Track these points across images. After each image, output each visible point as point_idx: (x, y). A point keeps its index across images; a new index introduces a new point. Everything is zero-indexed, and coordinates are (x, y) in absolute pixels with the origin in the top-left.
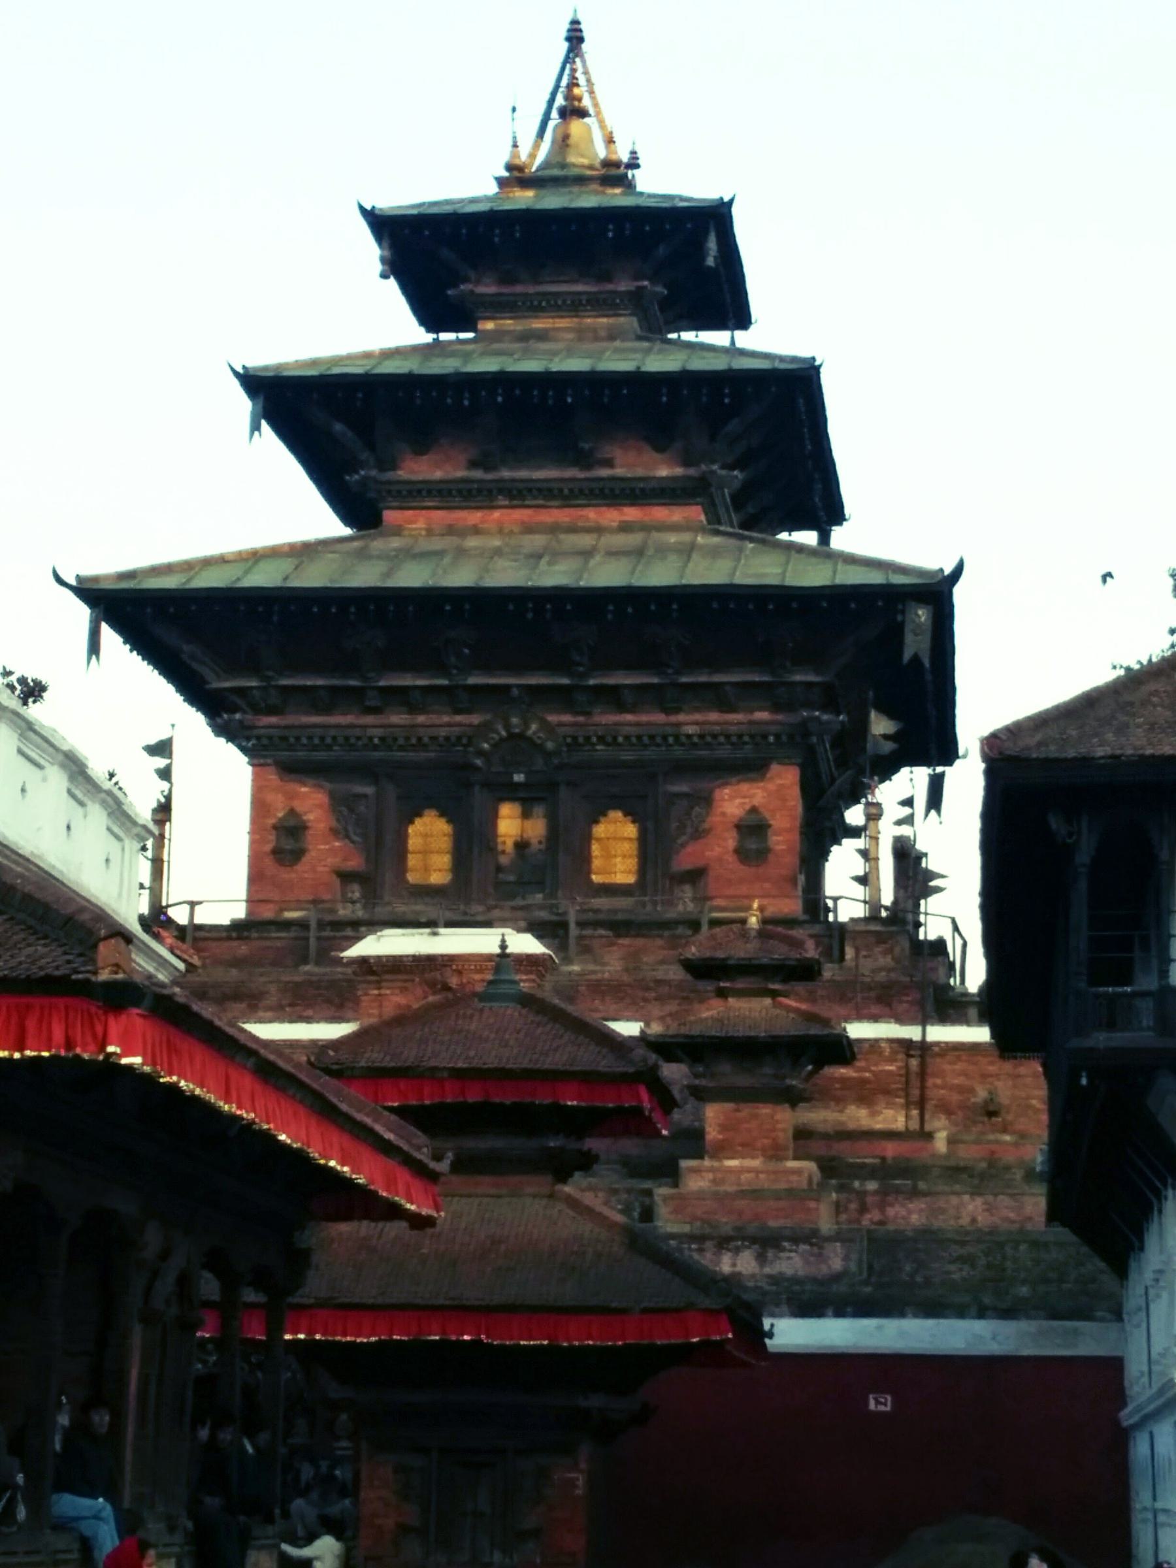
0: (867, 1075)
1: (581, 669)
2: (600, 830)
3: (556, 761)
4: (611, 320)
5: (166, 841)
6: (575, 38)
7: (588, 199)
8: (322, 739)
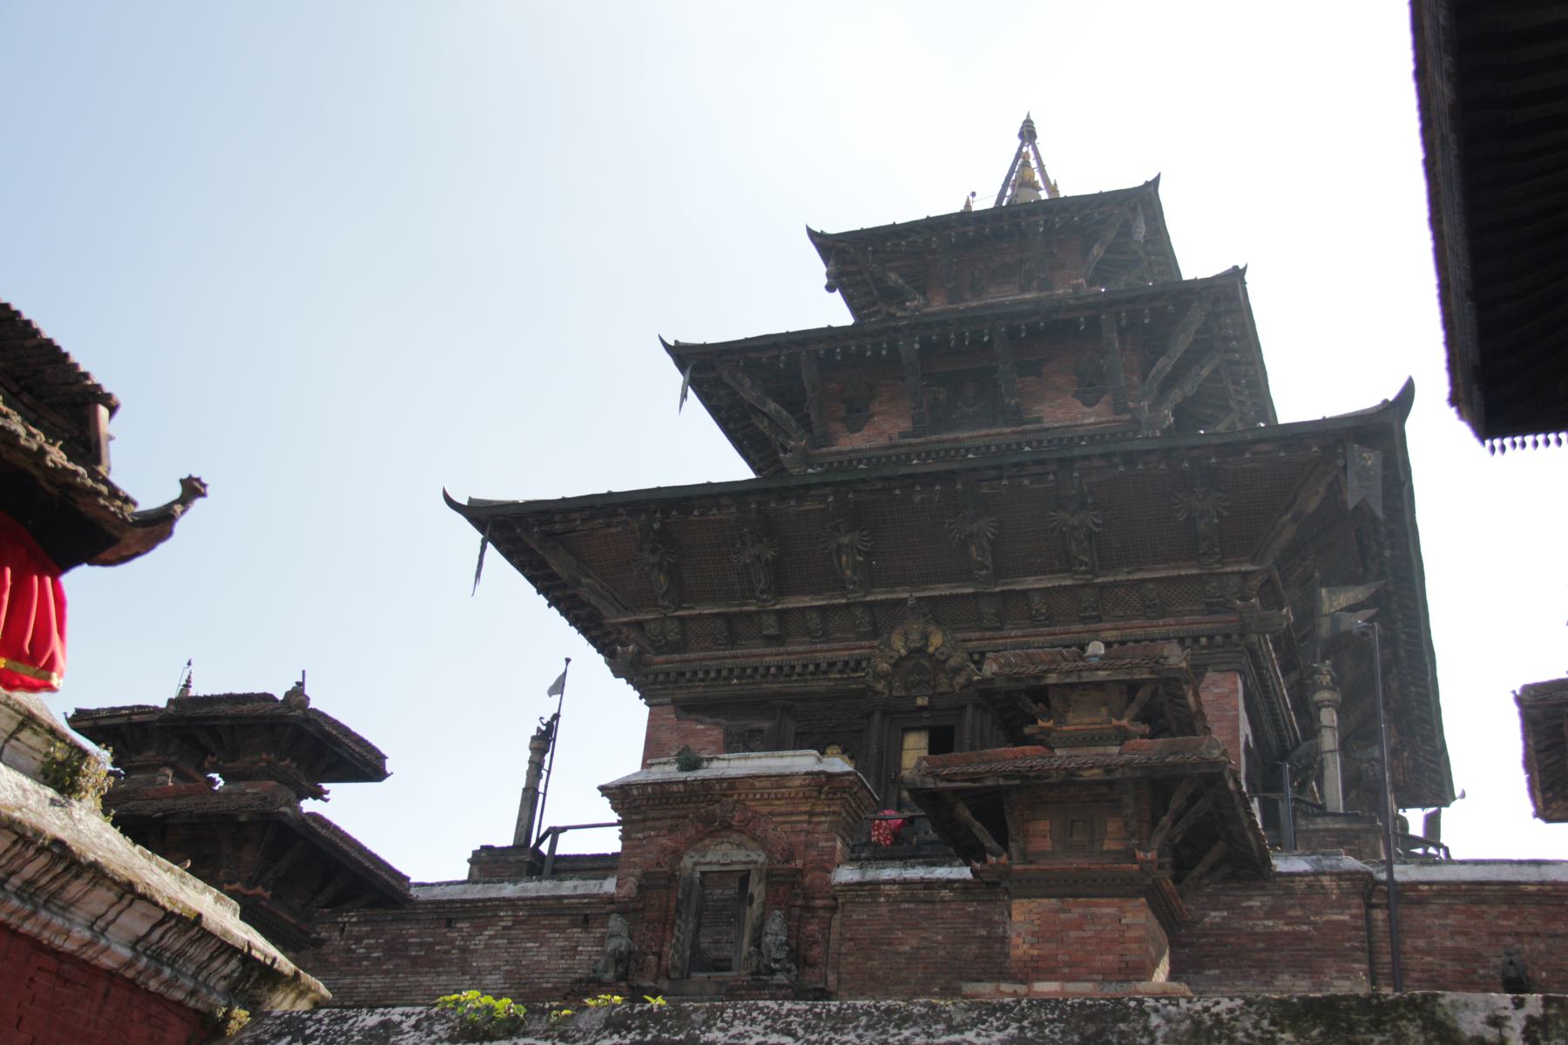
0: (1305, 928)
1: (984, 572)
5: (544, 773)
8: (719, 671)
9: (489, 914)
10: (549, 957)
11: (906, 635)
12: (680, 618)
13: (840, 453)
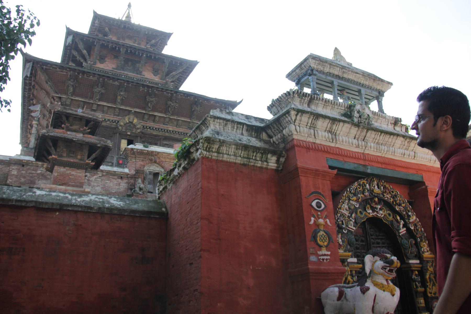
1: (150, 109)
3: (139, 131)
6: (129, 6)
9: (95, 172)
10: (113, 185)
11: (129, 118)
12: (72, 99)
13: (96, 67)
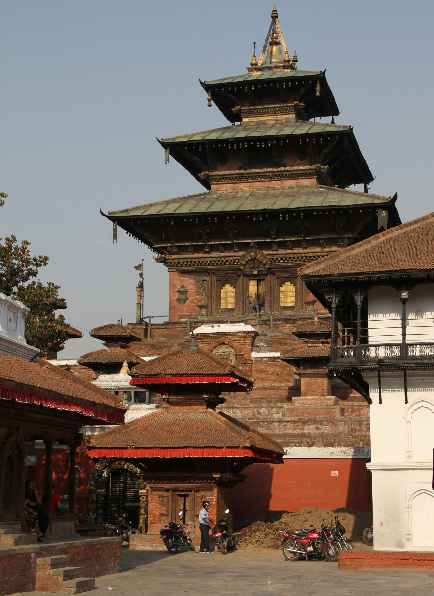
2: (282, 289)
3: (267, 267)
4: (287, 116)
5: (142, 297)
6: (275, 17)
7: (279, 74)
8: (191, 262)
